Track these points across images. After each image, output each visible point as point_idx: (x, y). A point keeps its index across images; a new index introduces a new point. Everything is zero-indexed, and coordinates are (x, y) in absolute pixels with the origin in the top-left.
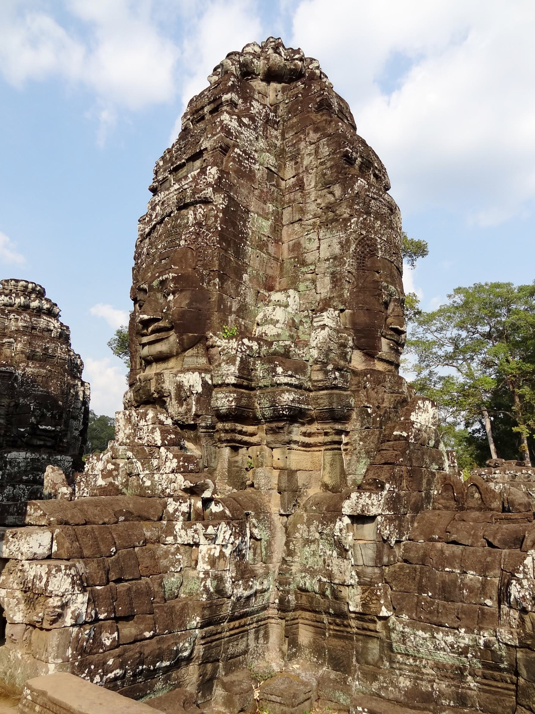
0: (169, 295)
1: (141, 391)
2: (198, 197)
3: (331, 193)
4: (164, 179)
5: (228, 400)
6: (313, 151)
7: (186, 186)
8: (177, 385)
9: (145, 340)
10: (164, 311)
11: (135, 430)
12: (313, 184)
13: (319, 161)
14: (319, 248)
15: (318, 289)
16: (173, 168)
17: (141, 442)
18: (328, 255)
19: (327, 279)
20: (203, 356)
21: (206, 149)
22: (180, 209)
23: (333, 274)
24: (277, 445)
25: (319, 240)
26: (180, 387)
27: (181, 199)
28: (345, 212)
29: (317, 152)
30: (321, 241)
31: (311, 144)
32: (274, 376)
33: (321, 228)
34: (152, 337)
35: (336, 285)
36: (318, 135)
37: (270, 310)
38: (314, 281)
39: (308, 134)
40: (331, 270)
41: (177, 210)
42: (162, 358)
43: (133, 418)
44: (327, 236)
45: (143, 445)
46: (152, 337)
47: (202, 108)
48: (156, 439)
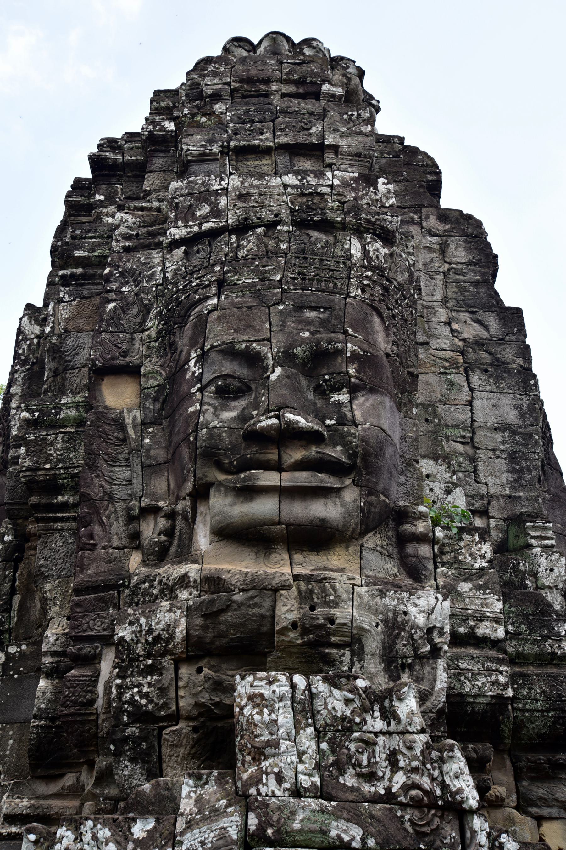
0: (337, 389)
1: (228, 616)
2: (368, 221)
3: (480, 322)
4: (203, 154)
5: (495, 683)
6: (437, 246)
7: (327, 190)
8: (386, 621)
9: (271, 479)
10: (328, 422)
11: (335, 747)
12: (438, 296)
13: (447, 266)
14: (470, 403)
15: (482, 474)
16: (235, 147)
17: (367, 788)
18: (492, 420)
19: (501, 464)
20: (390, 556)
21: (335, 148)
22: (303, 224)
23: (512, 457)
24: (554, 812)
25: (472, 390)
26: (395, 625)
27: (309, 207)
28: (514, 362)
29: (443, 250)
30: (476, 394)
31: (431, 233)
32: (545, 638)
33: (474, 372)
34: (304, 478)
35: (520, 478)
36: (448, 227)
37: (437, 491)
38: (473, 460)
39: (427, 217)
40: (508, 447)
41: (294, 223)
42: (316, 538)
43: (318, 704)
44: (488, 388)
45: (389, 797)
46: (304, 478)
47: (268, 81)
48: (455, 785)
